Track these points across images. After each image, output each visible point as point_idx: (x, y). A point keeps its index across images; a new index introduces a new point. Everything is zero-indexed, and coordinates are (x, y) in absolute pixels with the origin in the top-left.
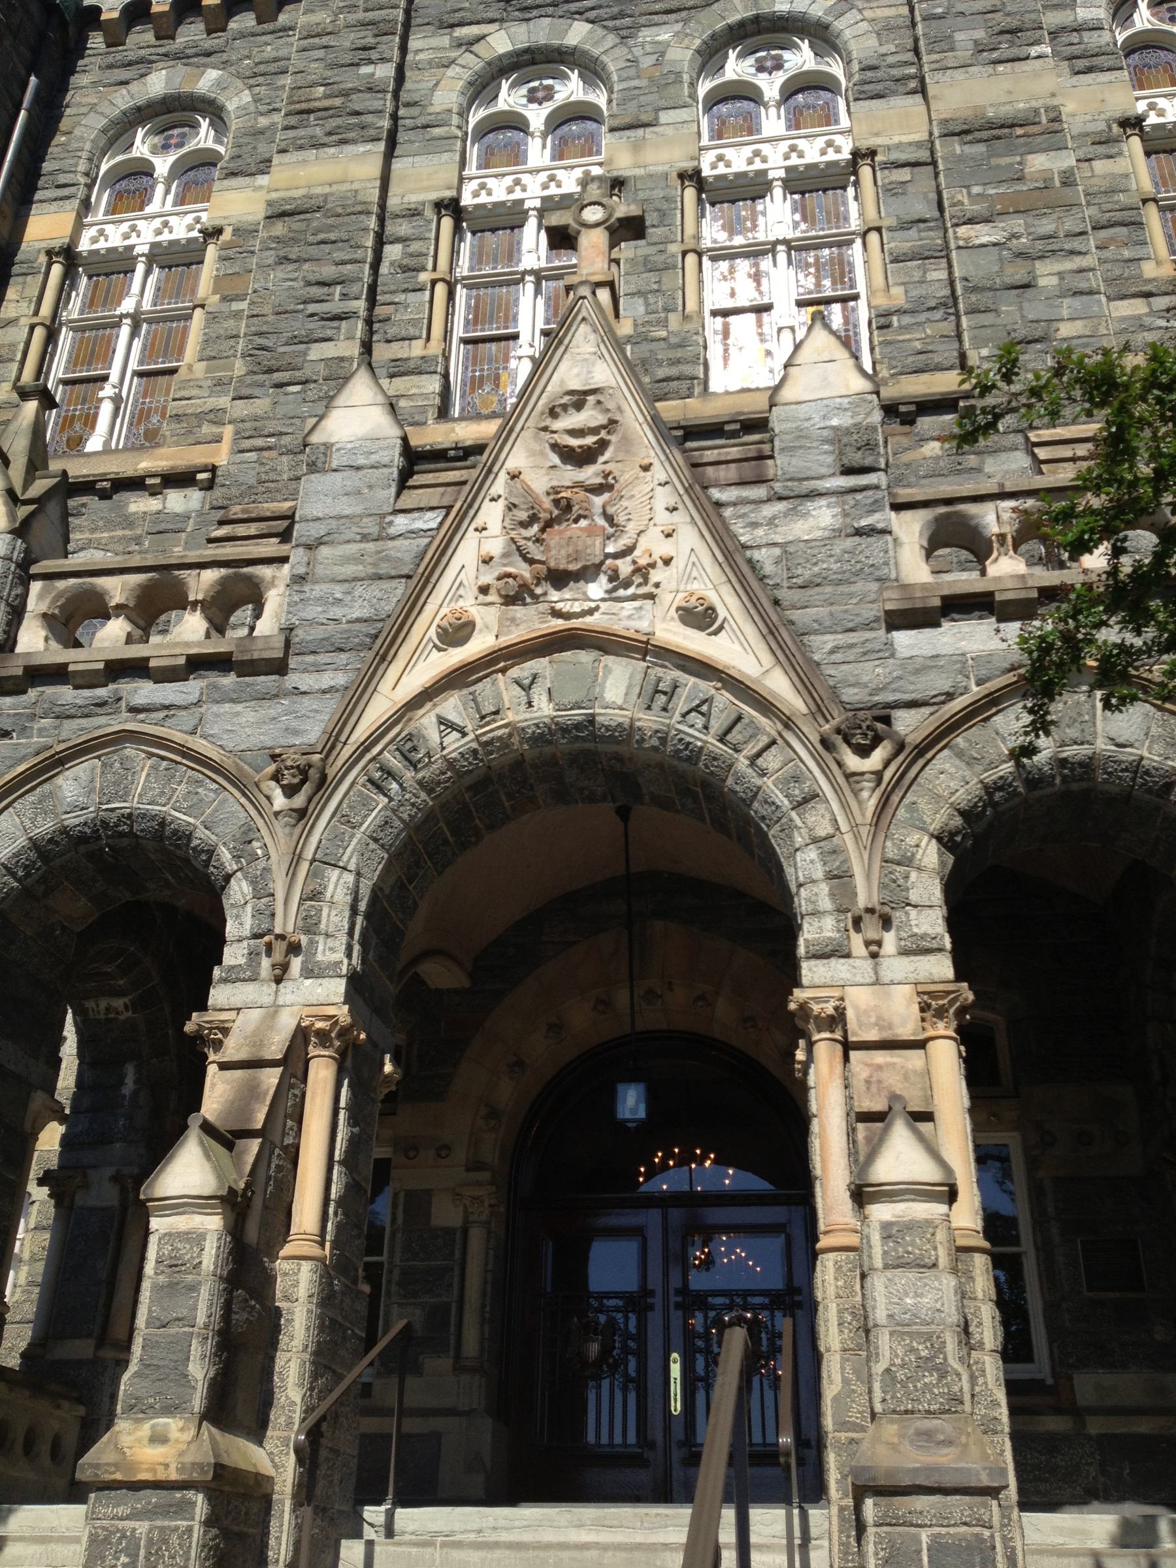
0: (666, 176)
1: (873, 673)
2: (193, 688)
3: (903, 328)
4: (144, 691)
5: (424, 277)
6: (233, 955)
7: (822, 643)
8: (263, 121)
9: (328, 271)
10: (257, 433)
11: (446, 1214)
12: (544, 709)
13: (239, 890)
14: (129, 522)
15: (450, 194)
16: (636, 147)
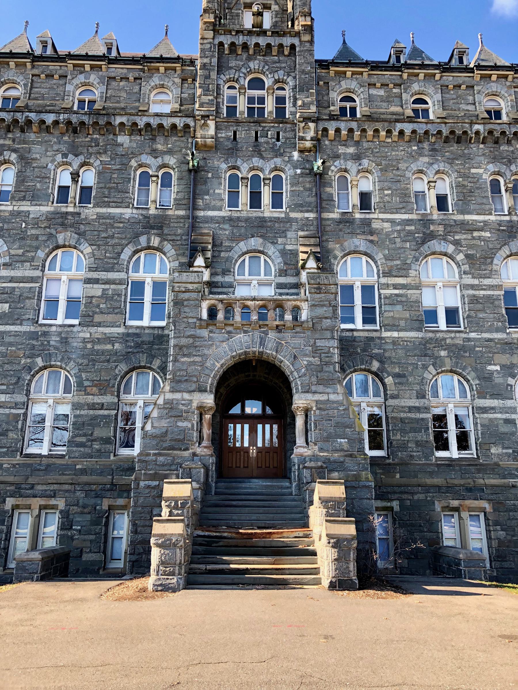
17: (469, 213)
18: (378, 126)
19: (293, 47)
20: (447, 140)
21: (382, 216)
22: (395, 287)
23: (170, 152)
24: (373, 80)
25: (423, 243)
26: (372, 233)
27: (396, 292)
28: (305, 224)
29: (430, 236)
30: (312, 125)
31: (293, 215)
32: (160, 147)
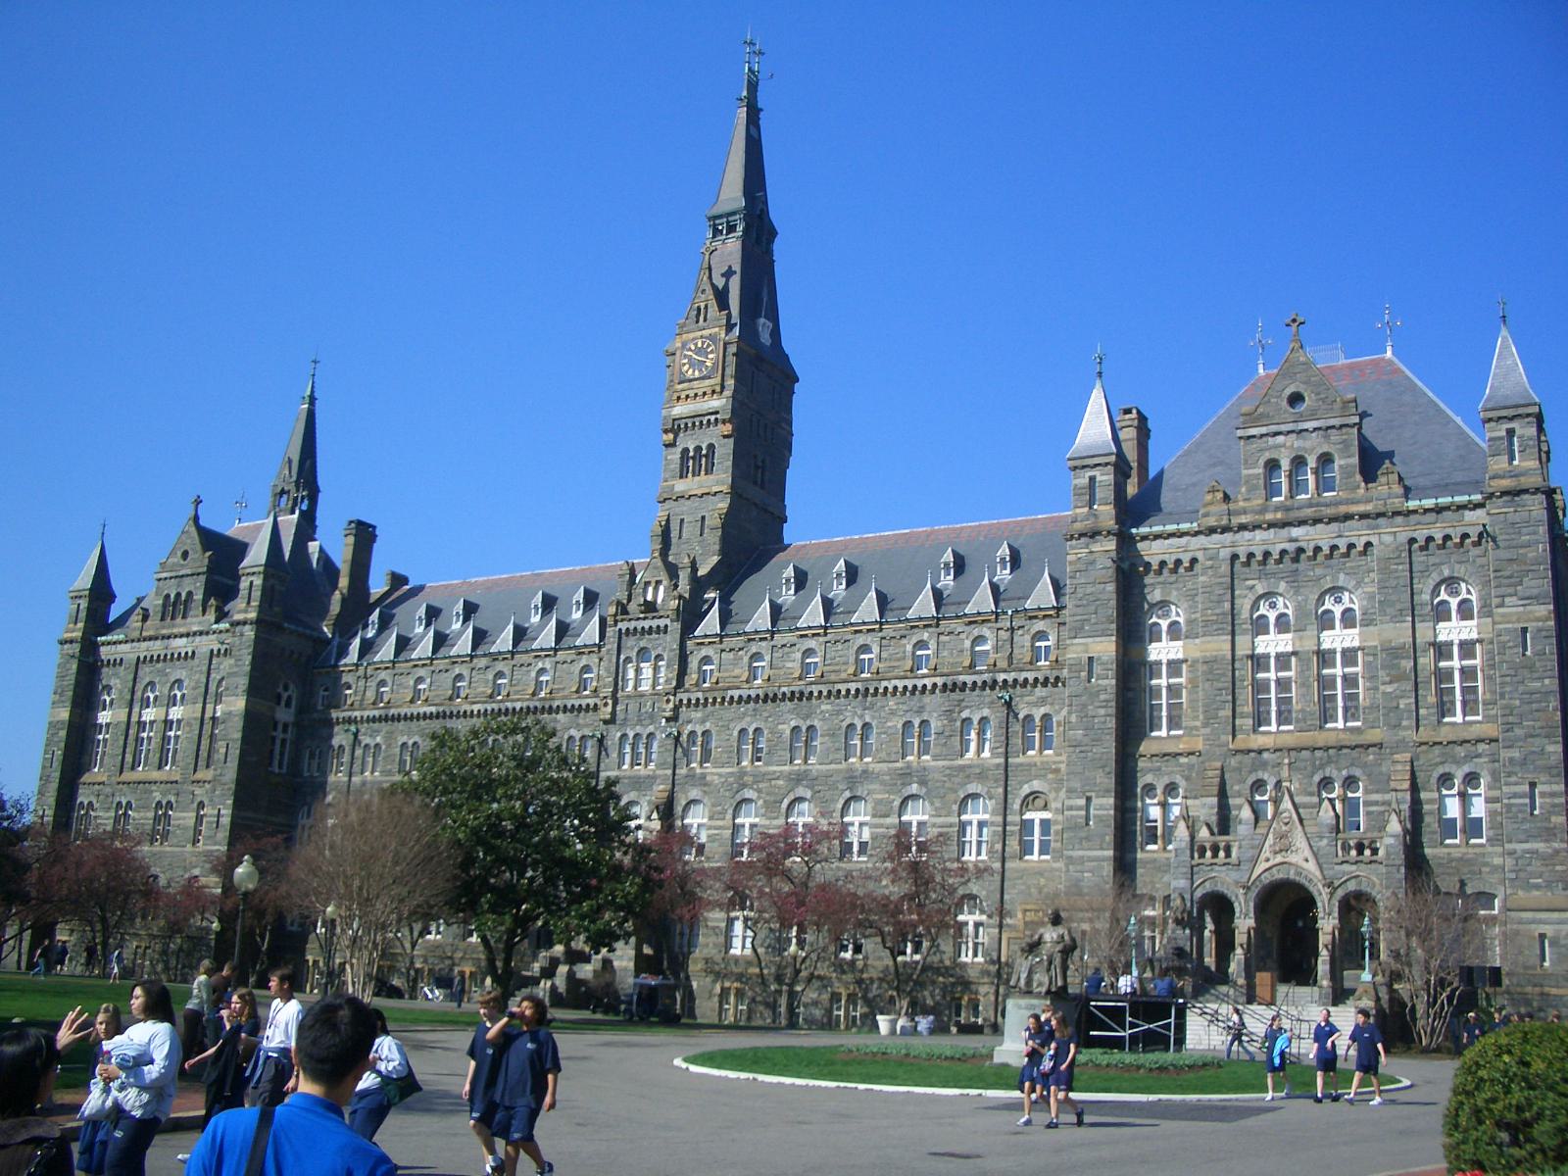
0: (1308, 652)
1: (1331, 872)
2: (1224, 868)
3: (1369, 713)
4: (1217, 868)
5: (1245, 683)
6: (1237, 915)
7: (1325, 866)
8: (1193, 616)
9: (1220, 685)
10: (1208, 740)
11: (1269, 935)
12: (1281, 876)
13: (1236, 905)
14: (1181, 765)
15: (1250, 652)
16: (1301, 638)
17: (772, 765)
18: (716, 694)
19: (666, 626)
20: (765, 701)
21: (714, 770)
22: (716, 828)
23: (587, 725)
24: (723, 646)
25: (738, 792)
26: (705, 785)
27: (716, 832)
28: (665, 777)
29: (744, 786)
30: (672, 698)
31: (658, 772)
32: (581, 721)
